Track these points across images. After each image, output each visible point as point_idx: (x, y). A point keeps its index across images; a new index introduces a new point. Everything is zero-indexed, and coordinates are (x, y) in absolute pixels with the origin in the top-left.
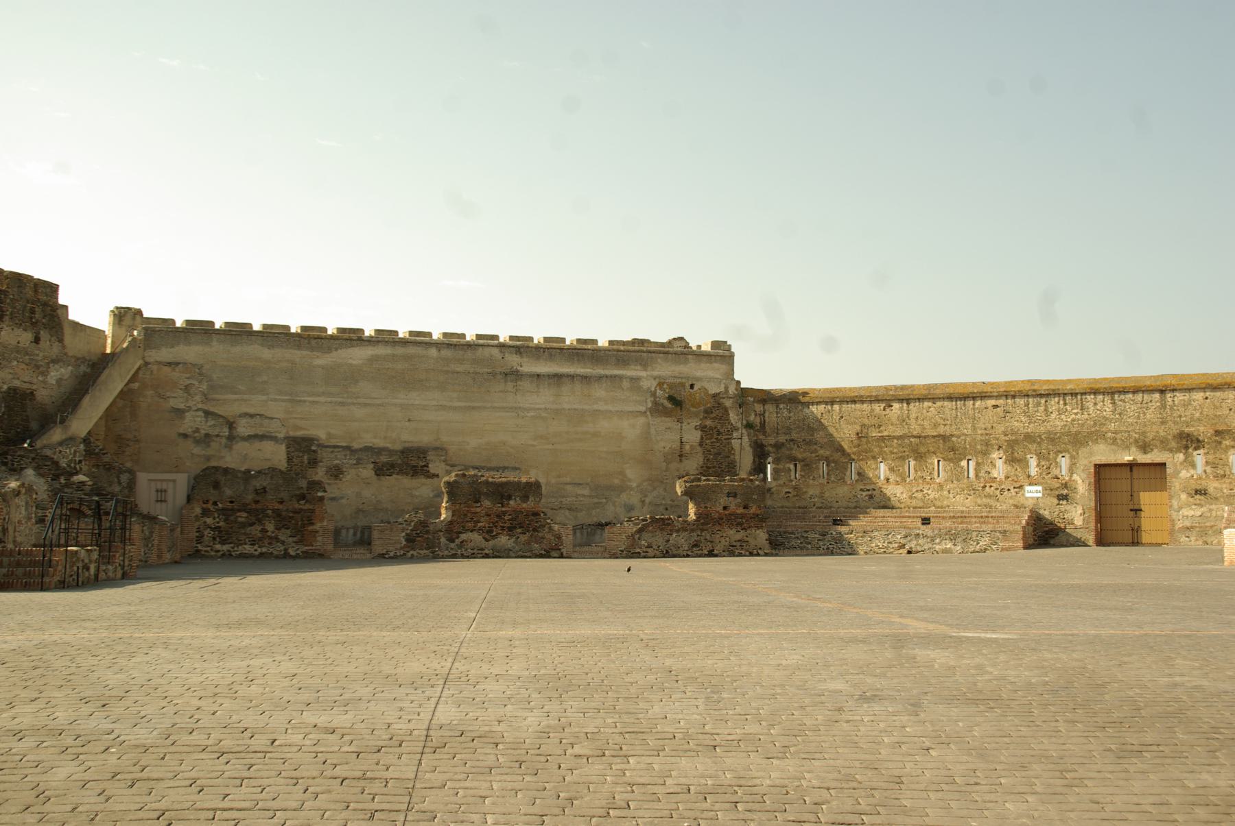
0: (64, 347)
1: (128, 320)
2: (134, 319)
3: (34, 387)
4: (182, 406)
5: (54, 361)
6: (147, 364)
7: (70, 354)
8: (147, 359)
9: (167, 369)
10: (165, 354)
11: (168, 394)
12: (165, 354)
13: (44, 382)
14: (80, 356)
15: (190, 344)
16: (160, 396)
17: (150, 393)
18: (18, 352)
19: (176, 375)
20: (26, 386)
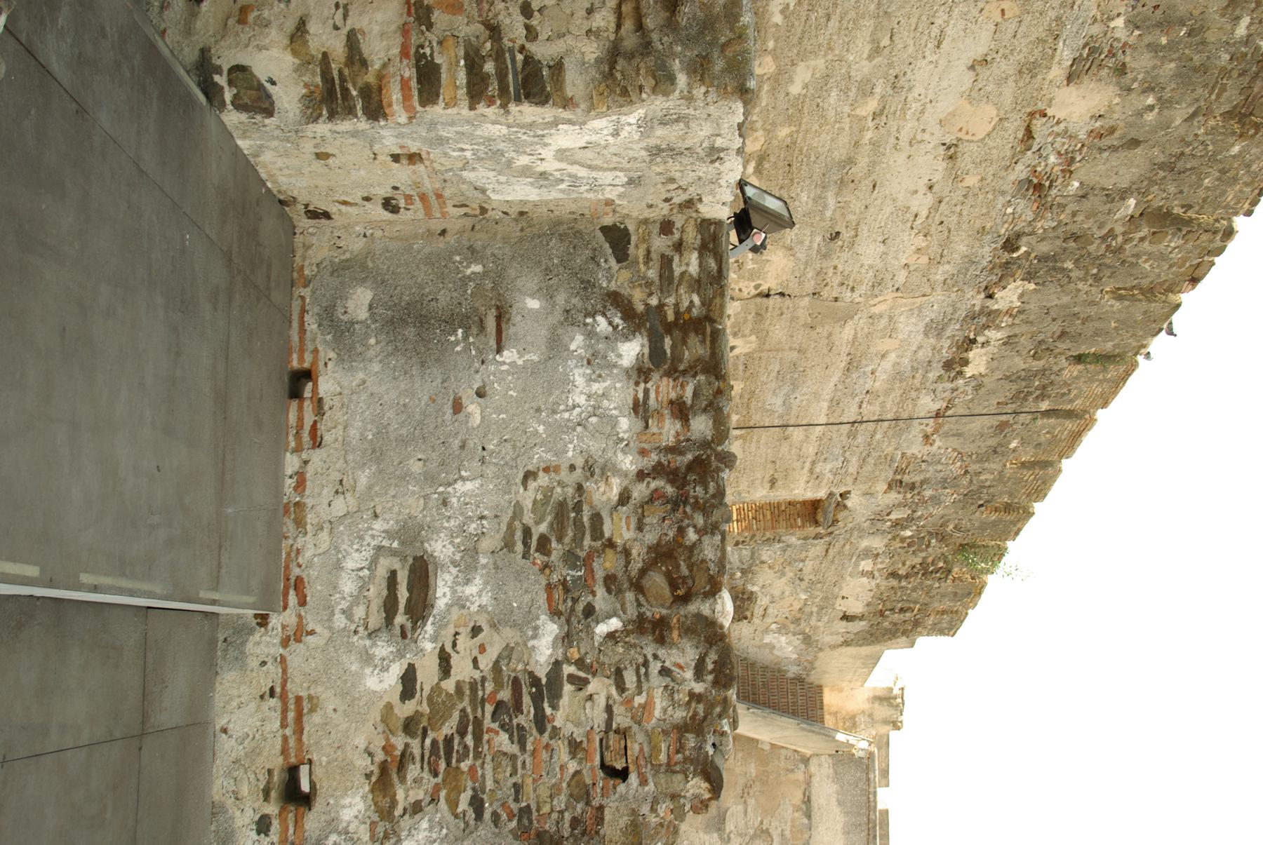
0: (833, 647)
1: (882, 712)
2: (886, 722)
3: (756, 621)
4: (730, 826)
5: (807, 640)
6: (806, 760)
7: (821, 654)
8: (814, 762)
9: (798, 797)
10: (826, 791)
11: (751, 801)
12: (826, 791)
13: (767, 631)
14: (817, 664)
15: (846, 833)
16: (747, 788)
17: (753, 769)
18: (826, 598)
19: (788, 812)
20: (758, 611)
